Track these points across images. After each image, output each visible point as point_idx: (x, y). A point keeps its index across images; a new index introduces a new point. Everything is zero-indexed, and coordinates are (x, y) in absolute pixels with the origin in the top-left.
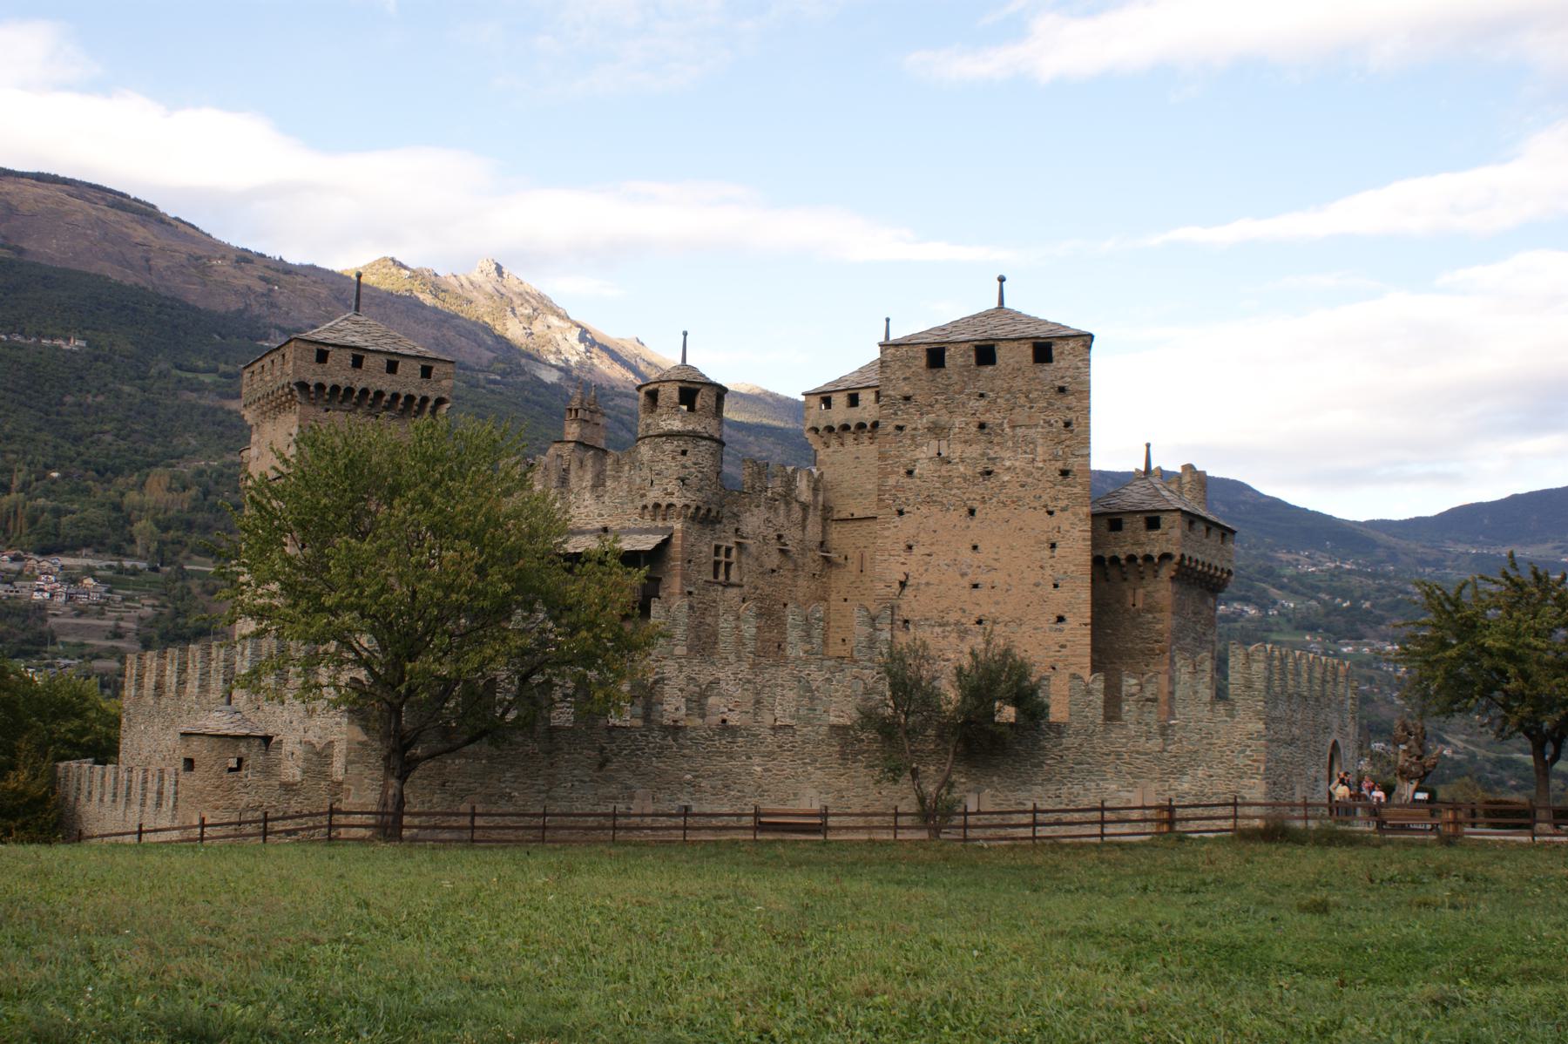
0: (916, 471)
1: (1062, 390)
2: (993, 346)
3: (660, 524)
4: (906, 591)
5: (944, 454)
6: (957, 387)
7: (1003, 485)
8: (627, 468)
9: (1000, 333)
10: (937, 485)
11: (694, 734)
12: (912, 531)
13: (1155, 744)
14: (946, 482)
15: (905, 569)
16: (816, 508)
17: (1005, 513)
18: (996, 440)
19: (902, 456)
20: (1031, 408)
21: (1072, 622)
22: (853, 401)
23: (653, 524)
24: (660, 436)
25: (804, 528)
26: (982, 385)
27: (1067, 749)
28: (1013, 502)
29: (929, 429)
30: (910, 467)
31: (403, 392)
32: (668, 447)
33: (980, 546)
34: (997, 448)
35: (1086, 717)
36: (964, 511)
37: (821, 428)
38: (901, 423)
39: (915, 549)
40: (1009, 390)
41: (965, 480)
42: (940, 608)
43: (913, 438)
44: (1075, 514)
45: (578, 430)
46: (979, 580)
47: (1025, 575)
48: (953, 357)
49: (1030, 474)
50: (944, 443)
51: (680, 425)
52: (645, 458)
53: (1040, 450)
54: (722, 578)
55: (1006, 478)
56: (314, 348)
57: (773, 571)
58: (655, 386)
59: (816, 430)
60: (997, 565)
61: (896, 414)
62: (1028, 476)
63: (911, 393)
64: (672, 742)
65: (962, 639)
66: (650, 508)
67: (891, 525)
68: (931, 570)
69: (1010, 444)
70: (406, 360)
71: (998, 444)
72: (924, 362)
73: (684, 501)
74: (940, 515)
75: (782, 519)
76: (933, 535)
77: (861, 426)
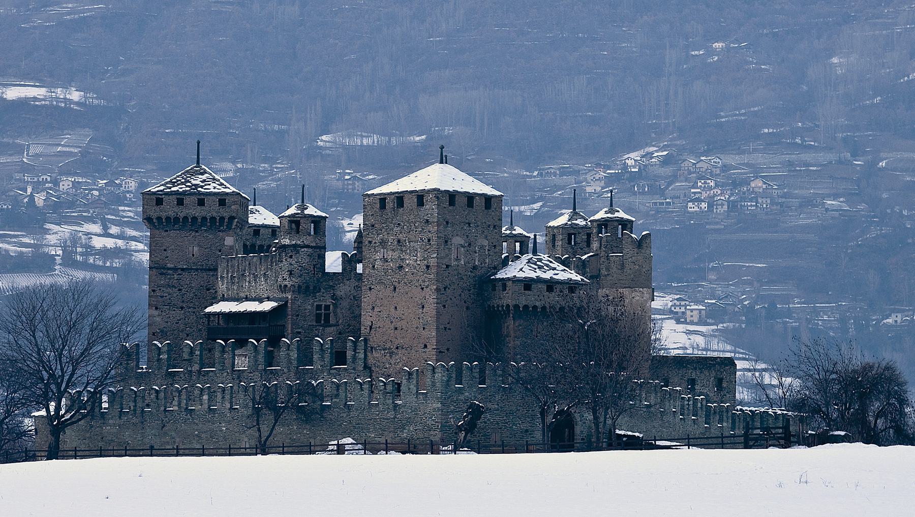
4: (373, 330)
11: (198, 413)
13: (391, 415)
15: (371, 319)
18: (404, 249)
20: (416, 231)
21: (430, 347)
27: (353, 417)
28: (409, 283)
35: (361, 402)
42: (384, 340)
44: (431, 290)
46: (399, 325)
48: (390, 205)
50: (385, 250)
55: (407, 270)
56: (154, 197)
61: (368, 234)
64: (189, 417)
65: (391, 356)
69: (408, 251)
70: (209, 197)
72: (378, 206)
76: (381, 301)
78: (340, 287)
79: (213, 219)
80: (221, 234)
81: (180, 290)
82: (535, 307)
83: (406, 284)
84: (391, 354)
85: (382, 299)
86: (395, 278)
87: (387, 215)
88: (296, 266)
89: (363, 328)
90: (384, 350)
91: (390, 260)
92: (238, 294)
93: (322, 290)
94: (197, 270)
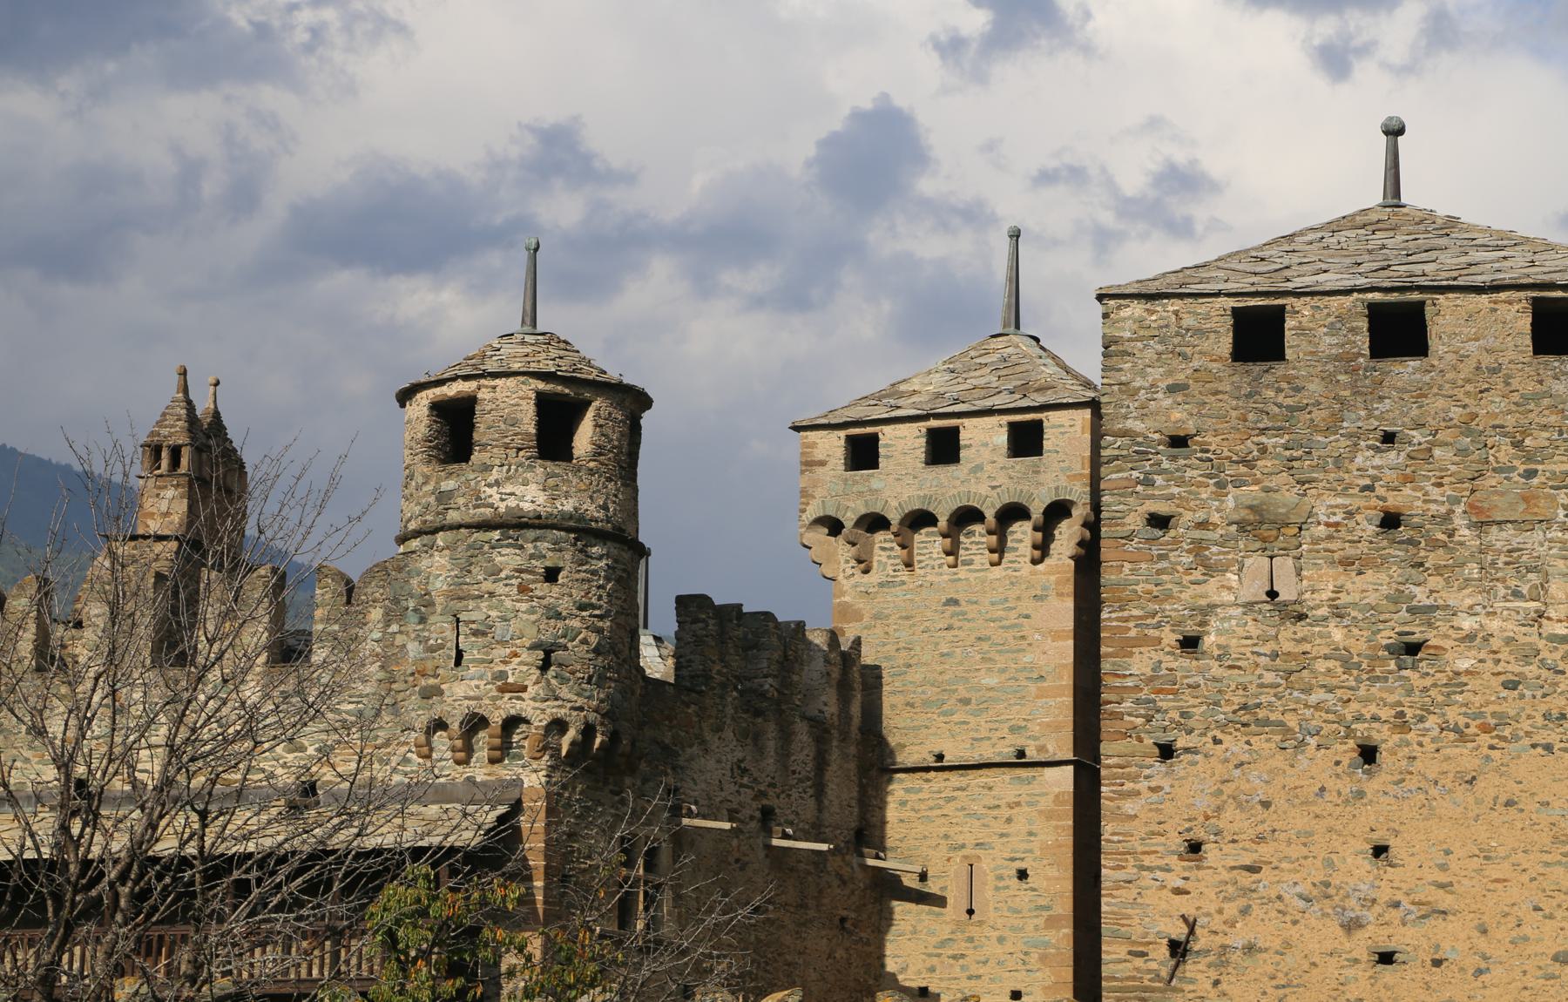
0: (1210, 640)
2: (1422, 304)
3: (480, 770)
4: (1190, 968)
5: (1285, 595)
6: (1318, 415)
7: (1456, 682)
8: (376, 614)
9: (1432, 270)
10: (1269, 677)
12: (1204, 803)
14: (1293, 669)
15: (1186, 905)
16: (845, 736)
17: (1465, 757)
18: (1433, 559)
19: (1169, 596)
20: (1531, 474)
22: (943, 448)
23: (459, 774)
24: (484, 526)
25: (820, 791)
26: (1389, 412)
28: (1486, 729)
29: (1242, 526)
30: (1191, 628)
32: (508, 558)
33: (1397, 847)
34: (1435, 582)
36: (1347, 751)
37: (849, 519)
38: (1162, 508)
39: (1210, 852)
40: (1466, 427)
41: (1347, 664)
45: (183, 506)
46: (1401, 938)
47: (1526, 930)
50: (1284, 565)
51: (541, 498)
52: (439, 585)
55: (1463, 665)
58: (468, 386)
59: (834, 526)
60: (1445, 900)
61: (1148, 483)
62: (1526, 658)
63: (1190, 427)
66: (455, 726)
67: (1143, 785)
68: (1257, 911)
69: (1472, 570)
71: (1438, 570)
72: (1225, 344)
73: (553, 710)
74: (1279, 761)
75: (770, 763)
77: (966, 516)
78: (692, 758)
83: (1456, 730)
85: (1266, 805)
86: (1366, 701)
87: (1298, 389)
88: (576, 623)
91: (1324, 611)
93: (643, 766)
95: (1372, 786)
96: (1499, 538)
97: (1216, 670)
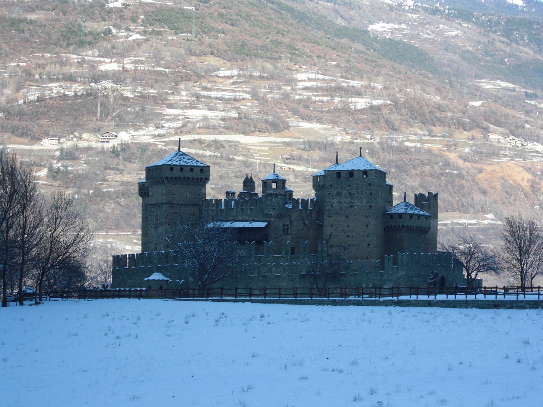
1: (370, 184)
7: (355, 210)
15: (331, 231)
18: (353, 197)
31: (195, 177)
32: (269, 198)
36: (345, 216)
39: (333, 227)
43: (333, 196)
44: (373, 218)
49: (361, 207)
53: (364, 200)
54: (286, 233)
57: (301, 229)
60: (353, 231)
65: (345, 250)
69: (357, 199)
72: (335, 176)
73: (274, 213)
79: (197, 179)
80: (200, 187)
81: (180, 215)
82: (414, 227)
84: (345, 249)
89: (324, 236)
90: (340, 247)
92: (226, 218)
94: (188, 205)
95: (347, 220)
96: (359, 195)
97: (334, 208)
